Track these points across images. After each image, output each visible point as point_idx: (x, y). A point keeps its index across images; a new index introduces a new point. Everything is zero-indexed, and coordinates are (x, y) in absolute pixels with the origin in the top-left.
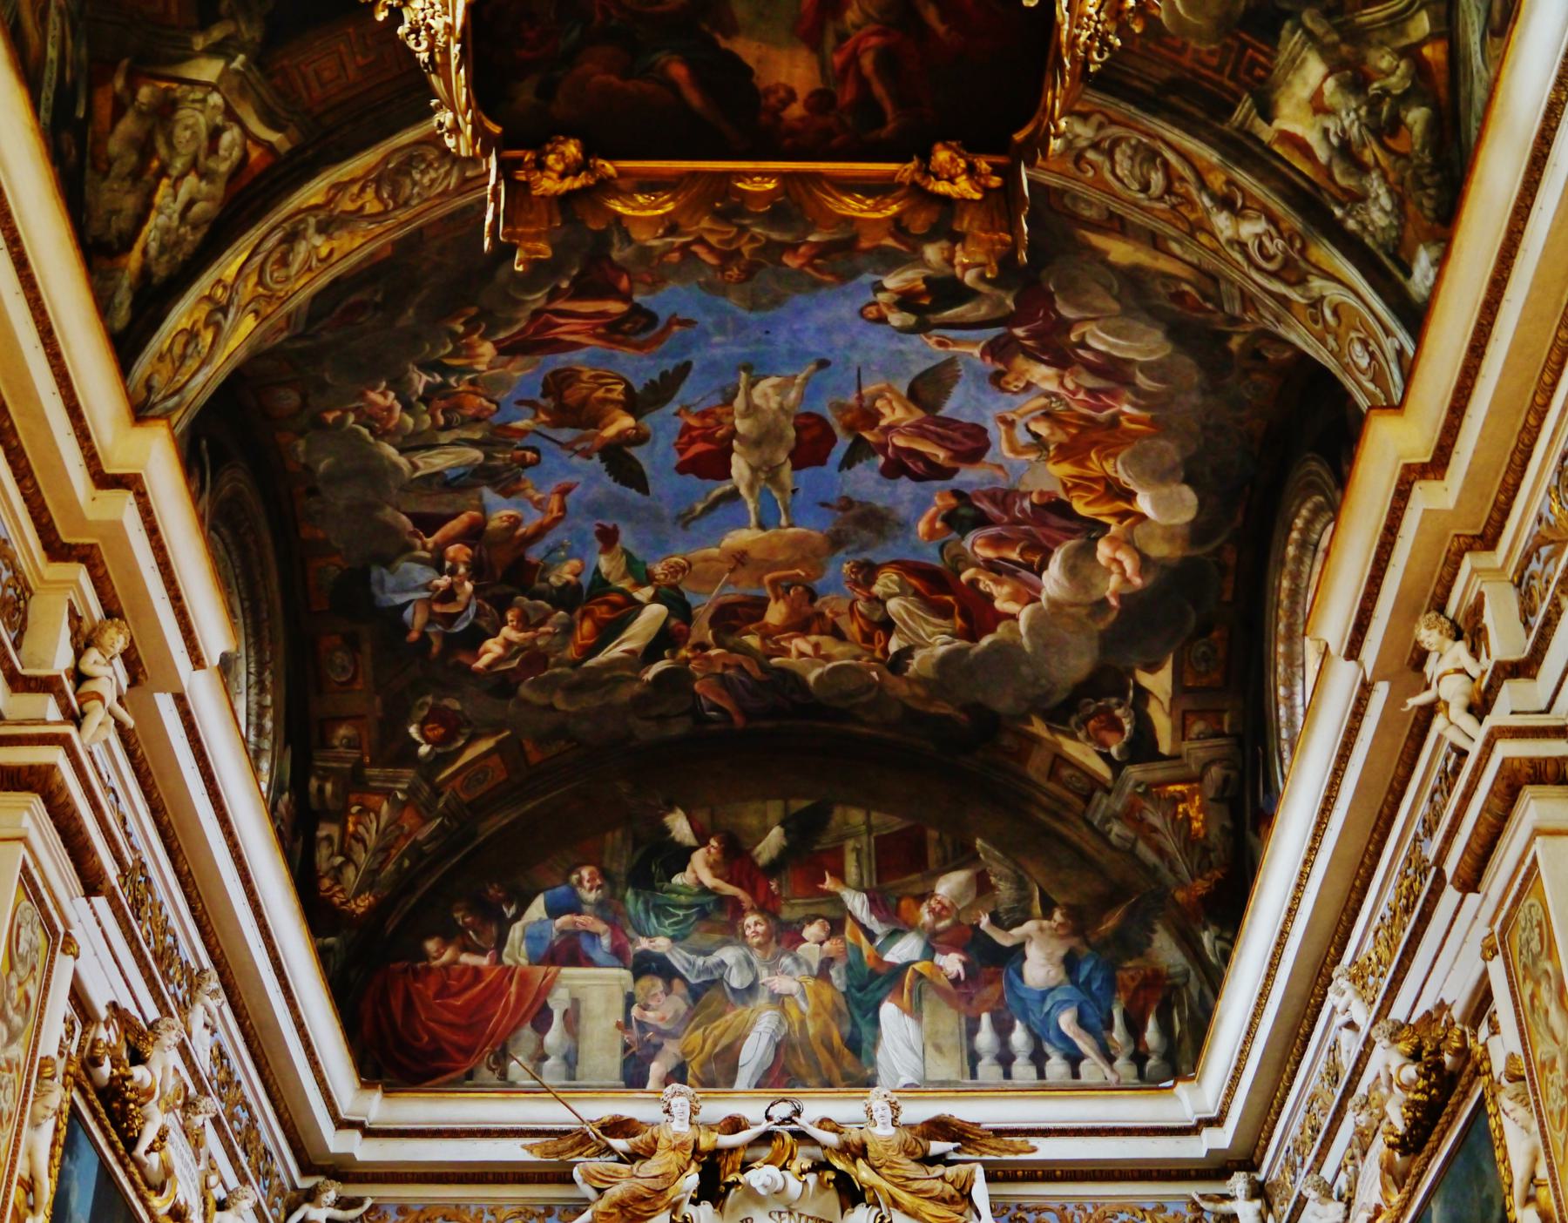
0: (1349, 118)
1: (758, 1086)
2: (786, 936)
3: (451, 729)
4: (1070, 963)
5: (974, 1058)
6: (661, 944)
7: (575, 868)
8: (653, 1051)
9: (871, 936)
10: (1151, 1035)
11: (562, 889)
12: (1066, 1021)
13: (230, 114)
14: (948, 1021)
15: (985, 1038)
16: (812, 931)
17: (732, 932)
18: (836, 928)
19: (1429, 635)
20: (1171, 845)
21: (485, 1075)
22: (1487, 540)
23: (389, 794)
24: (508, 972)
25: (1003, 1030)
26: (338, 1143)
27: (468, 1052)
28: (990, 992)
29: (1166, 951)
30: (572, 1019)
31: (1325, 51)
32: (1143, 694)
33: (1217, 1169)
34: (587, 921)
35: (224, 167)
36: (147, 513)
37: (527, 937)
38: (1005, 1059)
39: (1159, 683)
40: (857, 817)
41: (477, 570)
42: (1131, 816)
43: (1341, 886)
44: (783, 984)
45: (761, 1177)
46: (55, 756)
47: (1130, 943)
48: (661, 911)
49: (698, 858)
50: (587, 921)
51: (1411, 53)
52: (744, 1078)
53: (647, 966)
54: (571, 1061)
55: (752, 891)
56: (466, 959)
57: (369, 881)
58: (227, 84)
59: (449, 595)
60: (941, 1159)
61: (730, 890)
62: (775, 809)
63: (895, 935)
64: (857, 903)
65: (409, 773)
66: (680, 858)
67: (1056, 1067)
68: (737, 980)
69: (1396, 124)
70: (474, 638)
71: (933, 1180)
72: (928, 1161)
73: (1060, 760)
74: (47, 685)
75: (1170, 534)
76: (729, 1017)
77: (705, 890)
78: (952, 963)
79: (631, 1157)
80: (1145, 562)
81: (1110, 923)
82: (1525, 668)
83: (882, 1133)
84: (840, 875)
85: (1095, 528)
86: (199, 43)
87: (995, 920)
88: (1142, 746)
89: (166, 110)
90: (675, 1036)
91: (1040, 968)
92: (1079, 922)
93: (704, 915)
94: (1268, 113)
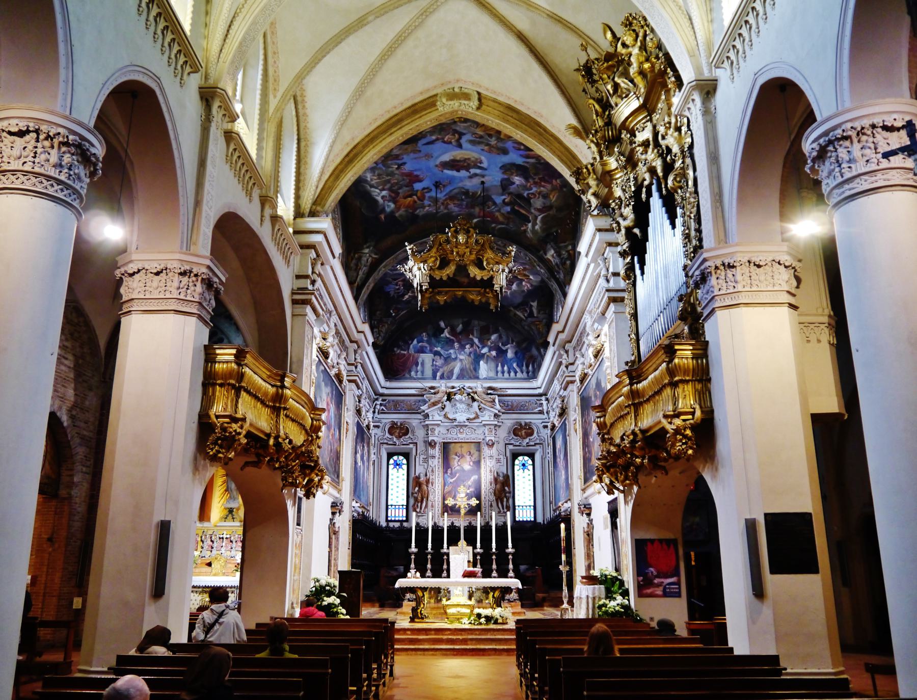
0: (557, 260)
1: (458, 378)
2: (462, 347)
3: (398, 310)
4: (516, 353)
5: (497, 372)
6: (439, 349)
7: (422, 333)
8: (438, 370)
9: (479, 347)
10: (530, 368)
11: (420, 338)
12: (515, 365)
13: (370, 256)
14: (492, 365)
15: (499, 368)
16: (468, 346)
17: (453, 347)
18: (472, 346)
19: (562, 352)
20: (536, 332)
21: (407, 375)
22: (570, 342)
23: (387, 323)
24: (410, 355)
25: (503, 367)
26: (381, 391)
27: (403, 371)
28: (501, 359)
29: (534, 352)
30: (423, 364)
31: (554, 249)
32: (531, 306)
33: (540, 395)
34: (425, 344)
35: (369, 264)
36: (365, 336)
37: (413, 347)
38: (503, 372)
39: (535, 304)
40: (476, 322)
41: (403, 285)
42: (529, 326)
43: (555, 370)
44: (462, 357)
45: (458, 397)
46: (356, 378)
47: (527, 349)
48: (439, 342)
49: (446, 331)
50: (425, 344)
51: (568, 252)
52: (455, 377)
53: (437, 353)
54: (423, 372)
55: (456, 338)
56: (402, 352)
57: (383, 339)
58: (371, 252)
59: (398, 289)
60: (491, 394)
61: (452, 338)
62: (460, 321)
63: (483, 347)
64: (476, 341)
65: (391, 319)
66: (442, 331)
67: (512, 374)
68: (453, 356)
69: (565, 263)
70: (403, 295)
71: (488, 398)
72: (488, 394)
73: (515, 314)
74: (352, 364)
75: (536, 281)
76: (453, 364)
77: (448, 338)
78: (494, 353)
79: (435, 393)
80: (532, 285)
81: (524, 345)
82: (572, 364)
83: (479, 390)
84: (473, 334)
85: (522, 280)
86: (365, 246)
87: (502, 345)
88: (531, 314)
89: (360, 259)
90: (442, 367)
91: (510, 354)
92: (518, 345)
93: (447, 343)
94: (546, 255)
